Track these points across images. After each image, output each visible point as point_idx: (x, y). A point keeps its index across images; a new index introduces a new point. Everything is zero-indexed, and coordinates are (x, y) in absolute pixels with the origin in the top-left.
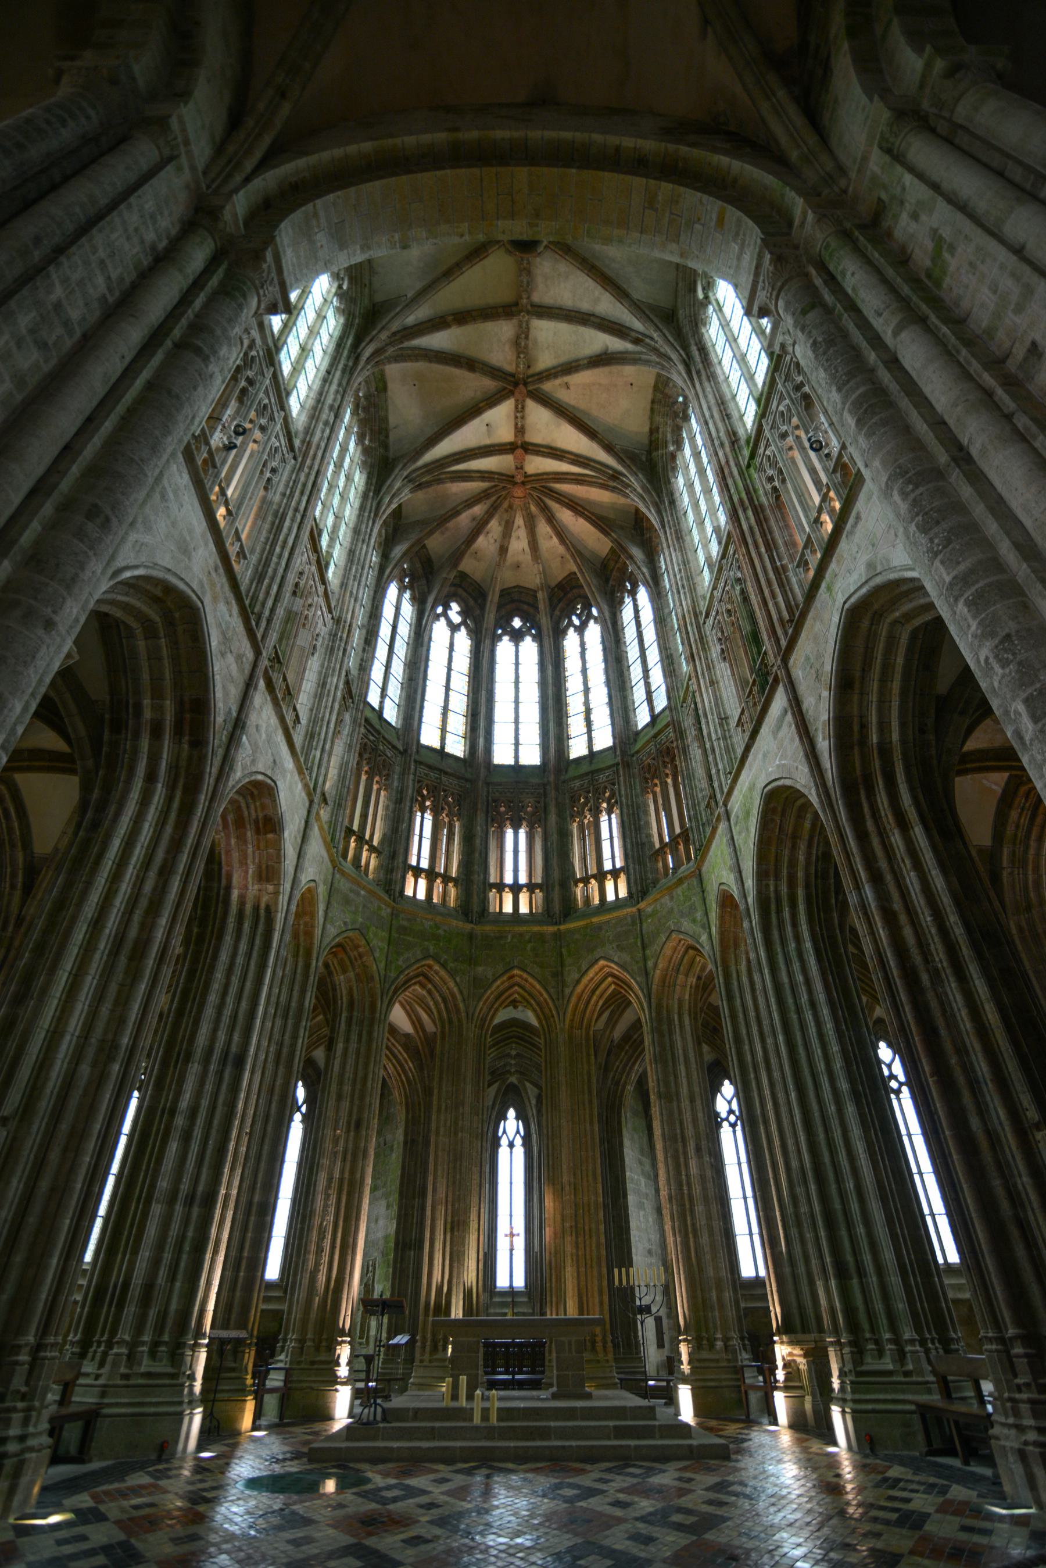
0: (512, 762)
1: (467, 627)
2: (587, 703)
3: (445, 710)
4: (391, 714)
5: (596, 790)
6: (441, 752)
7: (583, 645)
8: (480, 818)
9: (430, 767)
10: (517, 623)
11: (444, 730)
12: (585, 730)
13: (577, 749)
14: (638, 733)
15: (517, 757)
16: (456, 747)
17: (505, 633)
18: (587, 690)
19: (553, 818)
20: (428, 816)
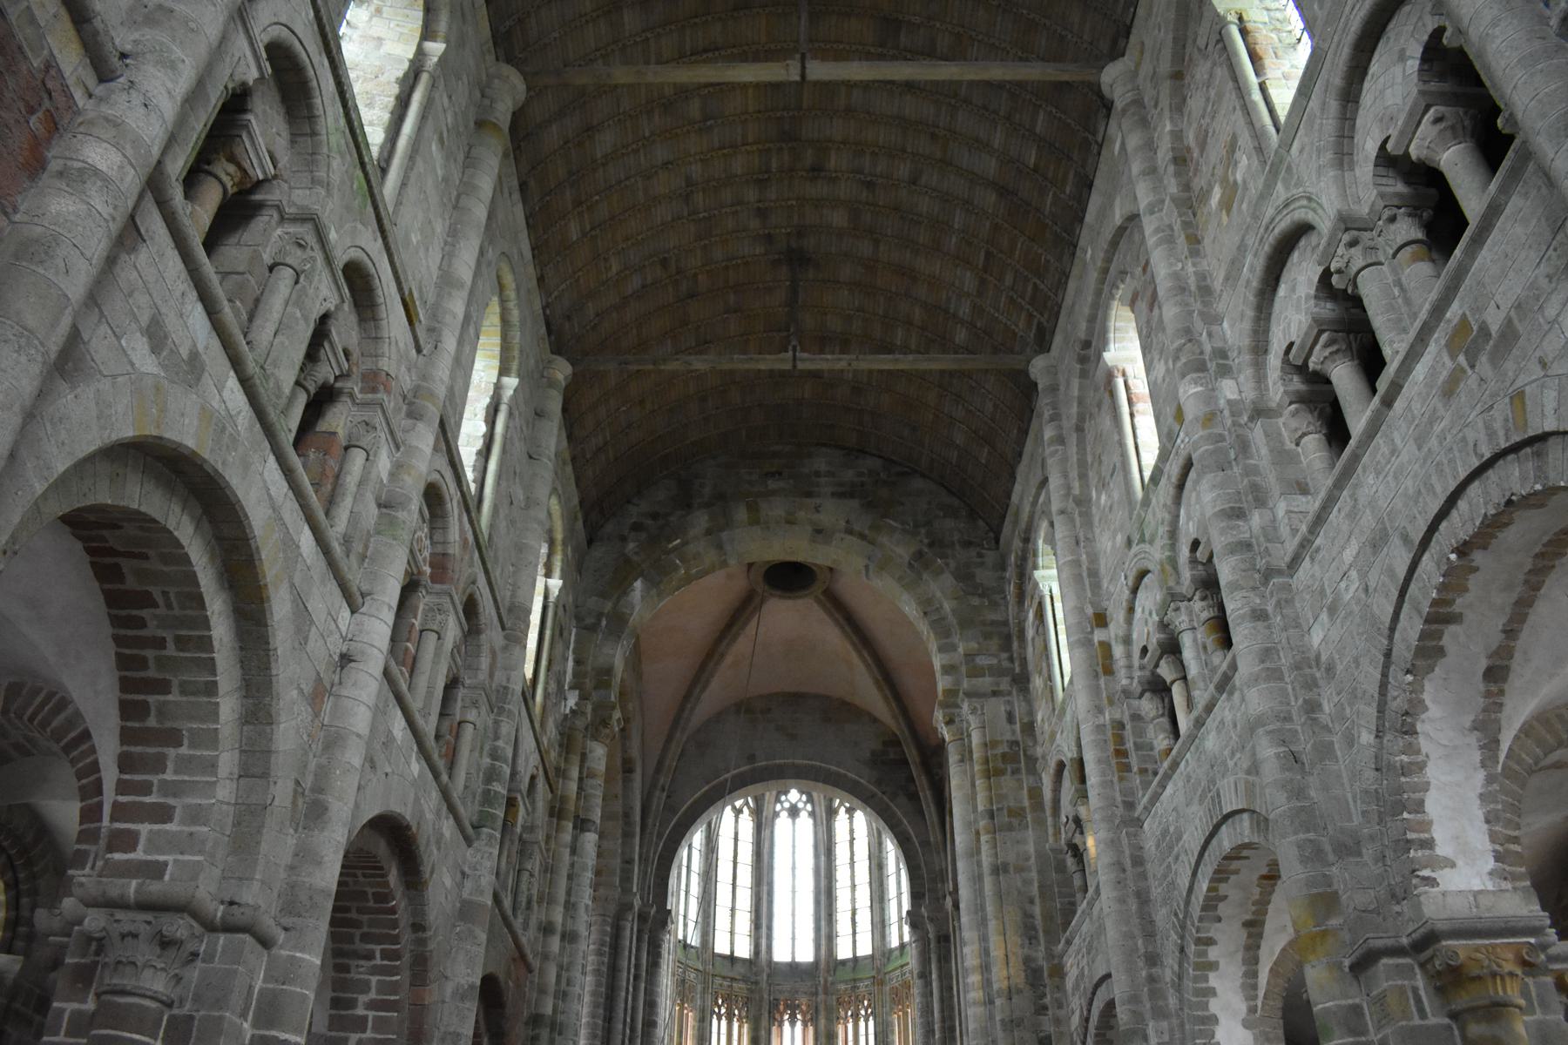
0: (788, 959)
1: (749, 807)
2: (853, 900)
3: (733, 910)
4: (694, 939)
5: (857, 997)
6: (732, 959)
7: (852, 831)
8: (764, 1023)
9: (724, 978)
10: (794, 795)
11: (732, 933)
12: (851, 931)
13: (843, 952)
14: (891, 951)
15: (793, 953)
16: (744, 950)
17: (783, 809)
18: (853, 887)
19: (822, 1022)
20: (724, 1022)
